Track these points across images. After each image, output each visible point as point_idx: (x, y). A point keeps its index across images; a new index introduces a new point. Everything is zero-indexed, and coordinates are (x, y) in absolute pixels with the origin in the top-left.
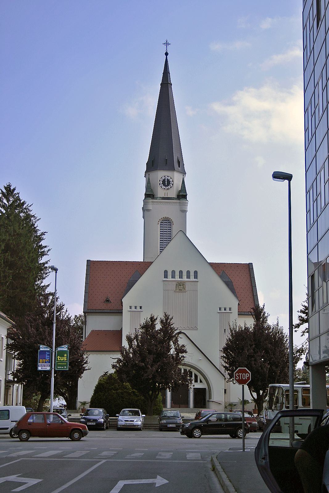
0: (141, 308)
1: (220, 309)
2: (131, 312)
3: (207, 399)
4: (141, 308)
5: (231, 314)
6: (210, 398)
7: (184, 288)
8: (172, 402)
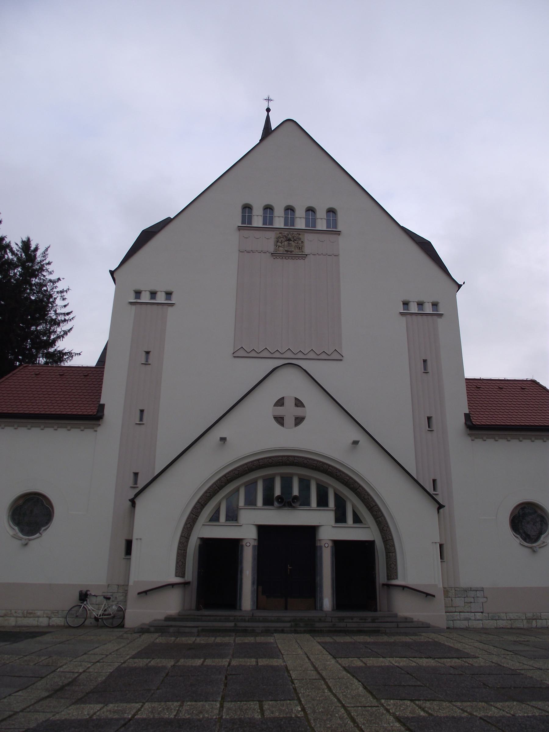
0: (169, 294)
1: (406, 304)
2: (138, 306)
3: (381, 577)
4: (169, 294)
5: (440, 320)
6: (392, 572)
7: (300, 248)
8: (260, 588)
